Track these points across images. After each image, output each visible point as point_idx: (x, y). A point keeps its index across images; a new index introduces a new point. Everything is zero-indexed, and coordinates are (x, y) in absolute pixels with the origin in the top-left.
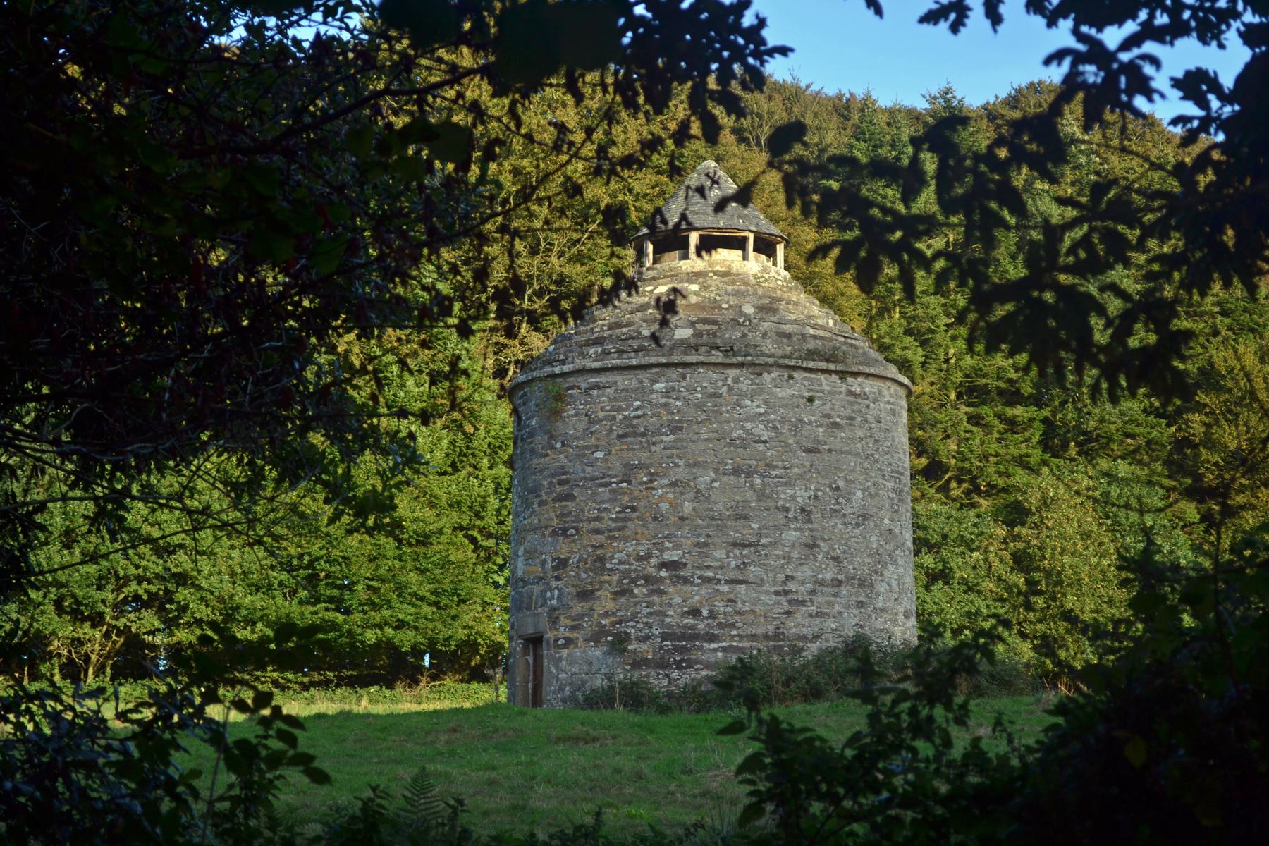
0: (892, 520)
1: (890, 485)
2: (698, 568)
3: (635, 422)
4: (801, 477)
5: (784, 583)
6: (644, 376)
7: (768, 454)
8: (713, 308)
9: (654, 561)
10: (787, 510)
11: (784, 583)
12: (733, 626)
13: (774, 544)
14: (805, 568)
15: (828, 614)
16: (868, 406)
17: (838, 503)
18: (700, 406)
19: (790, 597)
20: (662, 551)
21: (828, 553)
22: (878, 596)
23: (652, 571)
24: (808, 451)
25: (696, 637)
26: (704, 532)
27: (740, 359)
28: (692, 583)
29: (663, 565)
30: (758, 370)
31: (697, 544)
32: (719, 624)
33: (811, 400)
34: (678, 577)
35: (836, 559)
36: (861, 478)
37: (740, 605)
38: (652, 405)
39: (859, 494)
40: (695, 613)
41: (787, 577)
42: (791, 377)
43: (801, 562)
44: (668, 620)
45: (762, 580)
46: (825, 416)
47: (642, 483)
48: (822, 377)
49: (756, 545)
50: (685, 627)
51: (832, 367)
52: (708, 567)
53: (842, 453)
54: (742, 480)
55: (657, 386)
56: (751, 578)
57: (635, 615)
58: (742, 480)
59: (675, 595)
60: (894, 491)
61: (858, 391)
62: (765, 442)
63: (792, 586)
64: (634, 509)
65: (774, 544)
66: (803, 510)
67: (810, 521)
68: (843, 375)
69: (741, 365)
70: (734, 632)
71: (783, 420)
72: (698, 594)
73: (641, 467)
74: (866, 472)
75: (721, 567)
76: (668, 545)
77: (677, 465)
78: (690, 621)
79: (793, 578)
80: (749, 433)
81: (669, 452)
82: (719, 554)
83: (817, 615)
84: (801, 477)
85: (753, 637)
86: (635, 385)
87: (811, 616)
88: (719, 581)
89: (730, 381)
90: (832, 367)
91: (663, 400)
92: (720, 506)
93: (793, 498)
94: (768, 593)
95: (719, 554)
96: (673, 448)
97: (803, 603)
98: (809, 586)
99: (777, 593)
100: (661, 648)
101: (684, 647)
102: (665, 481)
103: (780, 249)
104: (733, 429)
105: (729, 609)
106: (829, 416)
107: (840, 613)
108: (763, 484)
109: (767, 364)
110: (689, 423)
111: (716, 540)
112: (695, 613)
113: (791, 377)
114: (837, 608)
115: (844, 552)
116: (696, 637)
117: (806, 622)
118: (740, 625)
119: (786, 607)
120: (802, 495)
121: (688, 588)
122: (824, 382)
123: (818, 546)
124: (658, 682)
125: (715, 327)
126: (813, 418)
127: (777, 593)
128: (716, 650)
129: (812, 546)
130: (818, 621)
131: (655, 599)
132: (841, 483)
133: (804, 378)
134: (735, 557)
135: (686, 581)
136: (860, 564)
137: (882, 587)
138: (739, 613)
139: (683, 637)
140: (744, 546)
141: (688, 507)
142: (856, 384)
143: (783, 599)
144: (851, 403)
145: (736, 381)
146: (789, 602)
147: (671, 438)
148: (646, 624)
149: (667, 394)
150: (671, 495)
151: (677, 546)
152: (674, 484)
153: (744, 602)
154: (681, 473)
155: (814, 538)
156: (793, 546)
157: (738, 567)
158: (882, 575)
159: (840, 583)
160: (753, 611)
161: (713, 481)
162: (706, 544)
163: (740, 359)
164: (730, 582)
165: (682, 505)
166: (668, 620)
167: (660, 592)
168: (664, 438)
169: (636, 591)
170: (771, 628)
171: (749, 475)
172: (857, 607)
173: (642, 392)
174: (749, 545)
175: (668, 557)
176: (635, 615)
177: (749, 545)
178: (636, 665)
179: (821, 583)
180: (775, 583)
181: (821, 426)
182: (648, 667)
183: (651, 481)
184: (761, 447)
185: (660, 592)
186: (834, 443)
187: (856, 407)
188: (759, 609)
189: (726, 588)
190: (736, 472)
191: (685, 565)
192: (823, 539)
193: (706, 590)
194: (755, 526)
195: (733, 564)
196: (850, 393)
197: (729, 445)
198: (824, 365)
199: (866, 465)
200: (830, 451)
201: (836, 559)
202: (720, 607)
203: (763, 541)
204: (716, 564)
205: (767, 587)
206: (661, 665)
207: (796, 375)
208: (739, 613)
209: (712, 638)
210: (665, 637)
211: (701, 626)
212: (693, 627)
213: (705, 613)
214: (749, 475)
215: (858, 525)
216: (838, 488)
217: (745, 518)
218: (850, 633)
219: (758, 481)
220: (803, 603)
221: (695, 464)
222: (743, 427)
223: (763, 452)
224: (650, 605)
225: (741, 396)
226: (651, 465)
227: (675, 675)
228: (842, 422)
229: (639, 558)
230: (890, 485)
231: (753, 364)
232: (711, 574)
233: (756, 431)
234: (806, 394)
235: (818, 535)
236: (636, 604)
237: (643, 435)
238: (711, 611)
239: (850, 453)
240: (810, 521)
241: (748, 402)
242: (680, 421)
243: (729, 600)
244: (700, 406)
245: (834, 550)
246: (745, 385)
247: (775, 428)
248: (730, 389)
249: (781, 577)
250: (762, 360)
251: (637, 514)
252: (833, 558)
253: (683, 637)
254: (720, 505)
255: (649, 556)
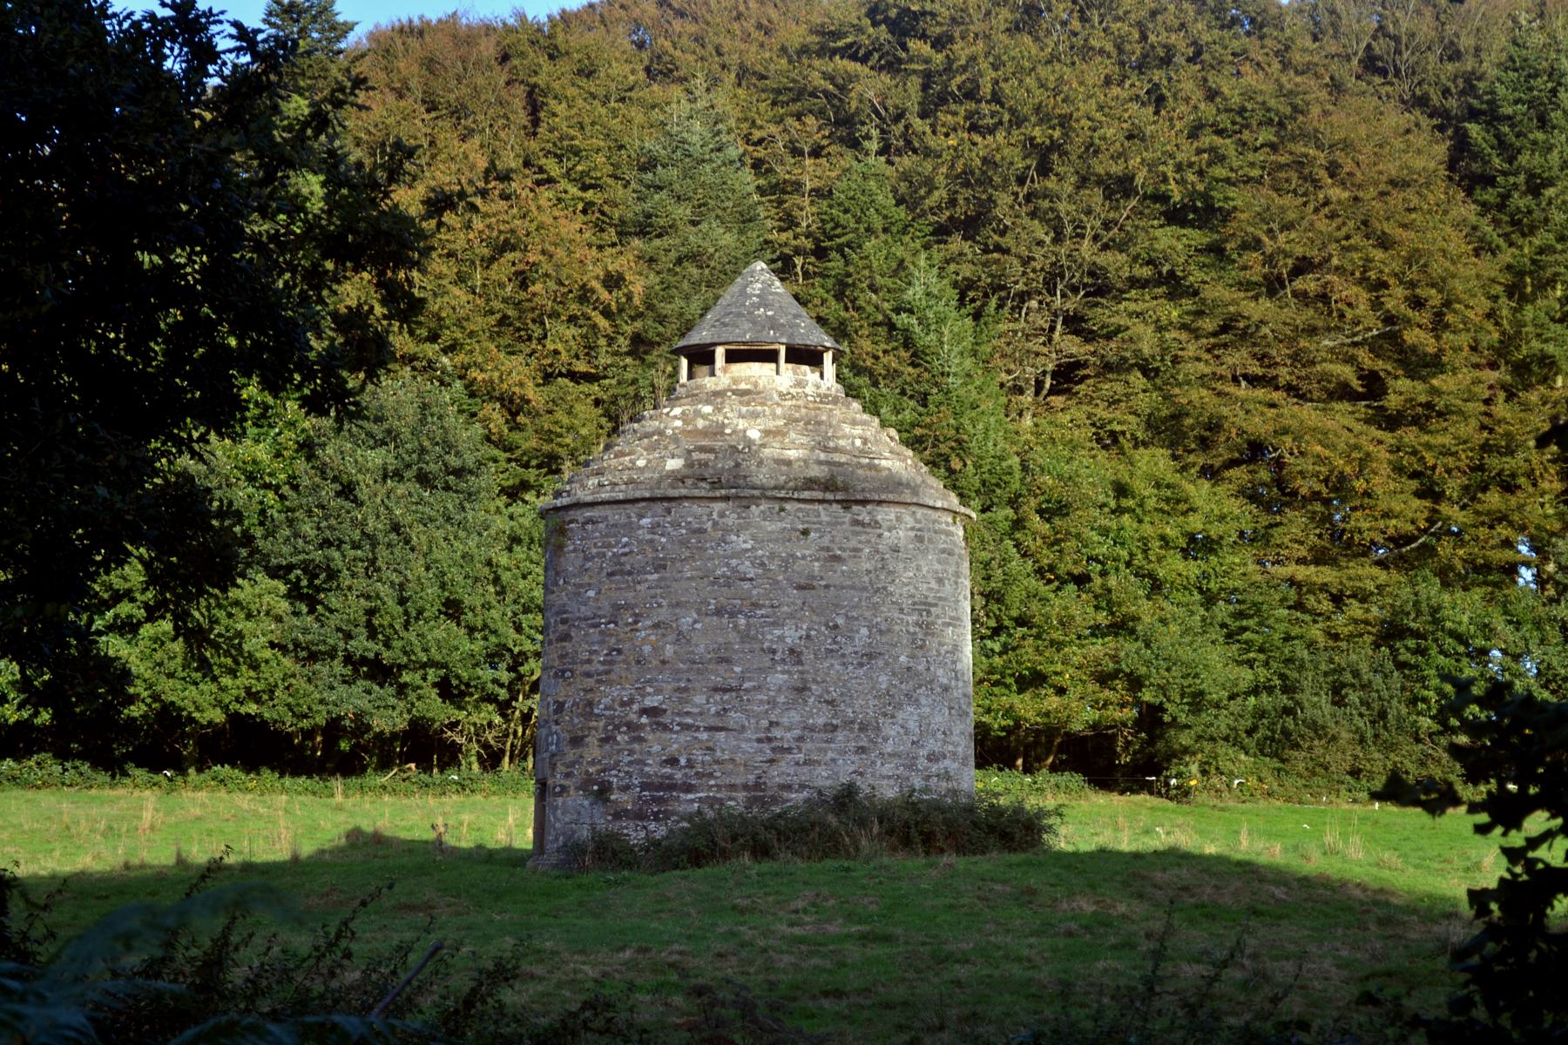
0: (912, 657)
1: (912, 618)
2: (678, 714)
3: (623, 559)
4: (791, 616)
5: (768, 730)
6: (632, 510)
7: (755, 592)
8: (715, 434)
9: (635, 707)
10: (774, 652)
11: (768, 730)
12: (711, 775)
13: (758, 688)
14: (793, 713)
15: (819, 763)
16: (880, 536)
17: (835, 643)
18: (684, 543)
19: (774, 744)
20: (643, 696)
21: (821, 696)
22: (886, 740)
23: (633, 717)
24: (800, 587)
25: (673, 787)
26: (685, 676)
27: (723, 492)
28: (671, 730)
29: (644, 711)
30: (745, 503)
31: (678, 689)
32: (697, 773)
33: (805, 533)
34: (658, 724)
35: (830, 703)
36: (868, 614)
37: (719, 753)
38: (640, 542)
39: (864, 631)
40: (673, 761)
41: (771, 723)
42: (782, 510)
43: (788, 707)
44: (647, 769)
45: (743, 727)
46: (822, 549)
47: (628, 624)
48: (821, 507)
49: (737, 689)
50: (662, 776)
51: (829, 496)
52: (688, 713)
53: (843, 588)
54: (725, 621)
55: (645, 521)
56: (731, 724)
57: (617, 763)
58: (725, 621)
59: (656, 744)
60: (917, 624)
61: (867, 520)
62: (751, 580)
63: (777, 733)
64: (619, 652)
65: (758, 688)
66: (792, 651)
67: (800, 663)
68: (846, 504)
69: (726, 498)
70: (712, 782)
71: (772, 556)
72: (676, 742)
73: (627, 607)
74: (875, 607)
75: (701, 714)
76: (649, 690)
77: (660, 606)
78: (667, 770)
79: (777, 724)
80: (734, 570)
81: (652, 592)
82: (700, 699)
83: (805, 763)
84: (791, 616)
85: (732, 787)
86: (624, 520)
87: (797, 764)
88: (698, 728)
89: (715, 516)
90: (829, 496)
91: (649, 537)
92: (701, 649)
93: (781, 638)
94: (750, 740)
95: (700, 699)
96: (657, 587)
97: (789, 750)
98: (797, 732)
99: (759, 741)
100: (640, 798)
101: (661, 798)
102: (649, 623)
103: (828, 358)
104: (716, 567)
105: (708, 758)
106: (828, 549)
107: (833, 760)
108: (748, 625)
109: (753, 497)
110: (673, 560)
111: (697, 685)
112: (673, 761)
113: (782, 510)
114: (830, 755)
115: (842, 694)
116: (673, 787)
117: (791, 771)
118: (718, 774)
119: (769, 754)
120: (791, 635)
121: (668, 736)
122: (822, 513)
123: (810, 689)
124: (635, 834)
125: (712, 456)
126: (807, 552)
127: (759, 741)
128: (692, 801)
129: (802, 690)
130: (805, 769)
131: (636, 746)
132: (840, 621)
133: (799, 510)
134: (716, 703)
135: (665, 728)
136: (863, 706)
137: (891, 730)
138: (717, 762)
139: (660, 787)
140: (725, 691)
141: (669, 650)
142: (863, 513)
143: (766, 747)
144: (857, 534)
145: (722, 515)
146: (773, 750)
147: (655, 576)
148: (627, 773)
149: (653, 529)
150: (653, 638)
151: (658, 691)
152: (656, 626)
153: (723, 751)
154: (664, 614)
155: (804, 681)
156: (779, 690)
157: (718, 713)
158: (893, 717)
159: (835, 728)
160: (732, 760)
161: (695, 622)
162: (686, 689)
163: (723, 492)
164: (710, 729)
165: (663, 648)
166: (647, 769)
167: (641, 740)
168: (650, 577)
169: (619, 738)
170: (752, 778)
171: (732, 615)
172: (856, 753)
173: (630, 528)
174: (731, 690)
175: (650, 702)
176: (617, 763)
177: (731, 690)
178: (617, 816)
179: (812, 729)
180: (757, 730)
181: (817, 560)
182: (628, 818)
183: (636, 622)
184: (747, 585)
185: (641, 740)
186: (834, 577)
187: (863, 538)
188: (739, 758)
189: (704, 736)
190: (719, 612)
191: (665, 711)
192: (814, 681)
193: (685, 737)
194: (737, 669)
195: (713, 710)
196: (856, 523)
197: (713, 584)
198: (818, 495)
199: (876, 599)
200: (827, 587)
201: (830, 703)
202: (699, 755)
203: (746, 685)
204: (695, 710)
205: (749, 734)
206: (640, 816)
207: (788, 506)
208: (717, 762)
209: (689, 788)
210: (644, 786)
211: (679, 776)
212: (670, 777)
213: (683, 762)
214: (732, 615)
215: (861, 665)
216: (836, 627)
217: (727, 661)
218: (844, 780)
219: (742, 621)
220: (789, 750)
221: (678, 604)
222: (727, 565)
223: (750, 590)
224: (631, 752)
225: (727, 530)
226: (636, 605)
227: (652, 826)
228: (844, 555)
229: (623, 704)
230: (912, 618)
231: (738, 497)
232: (689, 721)
233: (741, 568)
234: (801, 527)
235: (809, 677)
236: (619, 751)
237: (630, 573)
238: (689, 760)
239: (853, 587)
240: (800, 663)
241: (734, 538)
242: (664, 559)
243: (708, 749)
244: (684, 543)
245: (829, 693)
246: (731, 519)
247: (762, 564)
248: (715, 524)
249: (764, 723)
250: (748, 492)
251: (621, 657)
252: (828, 702)
253: (660, 787)
254: (701, 648)
255: (631, 701)
